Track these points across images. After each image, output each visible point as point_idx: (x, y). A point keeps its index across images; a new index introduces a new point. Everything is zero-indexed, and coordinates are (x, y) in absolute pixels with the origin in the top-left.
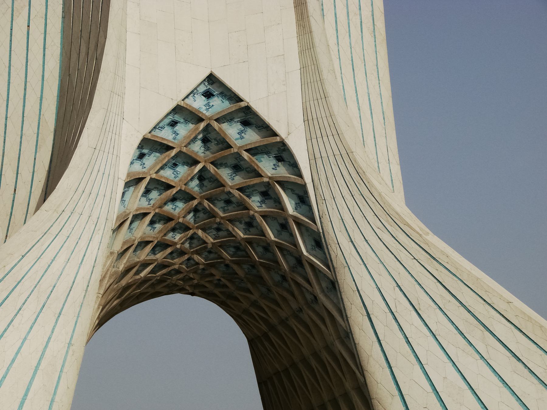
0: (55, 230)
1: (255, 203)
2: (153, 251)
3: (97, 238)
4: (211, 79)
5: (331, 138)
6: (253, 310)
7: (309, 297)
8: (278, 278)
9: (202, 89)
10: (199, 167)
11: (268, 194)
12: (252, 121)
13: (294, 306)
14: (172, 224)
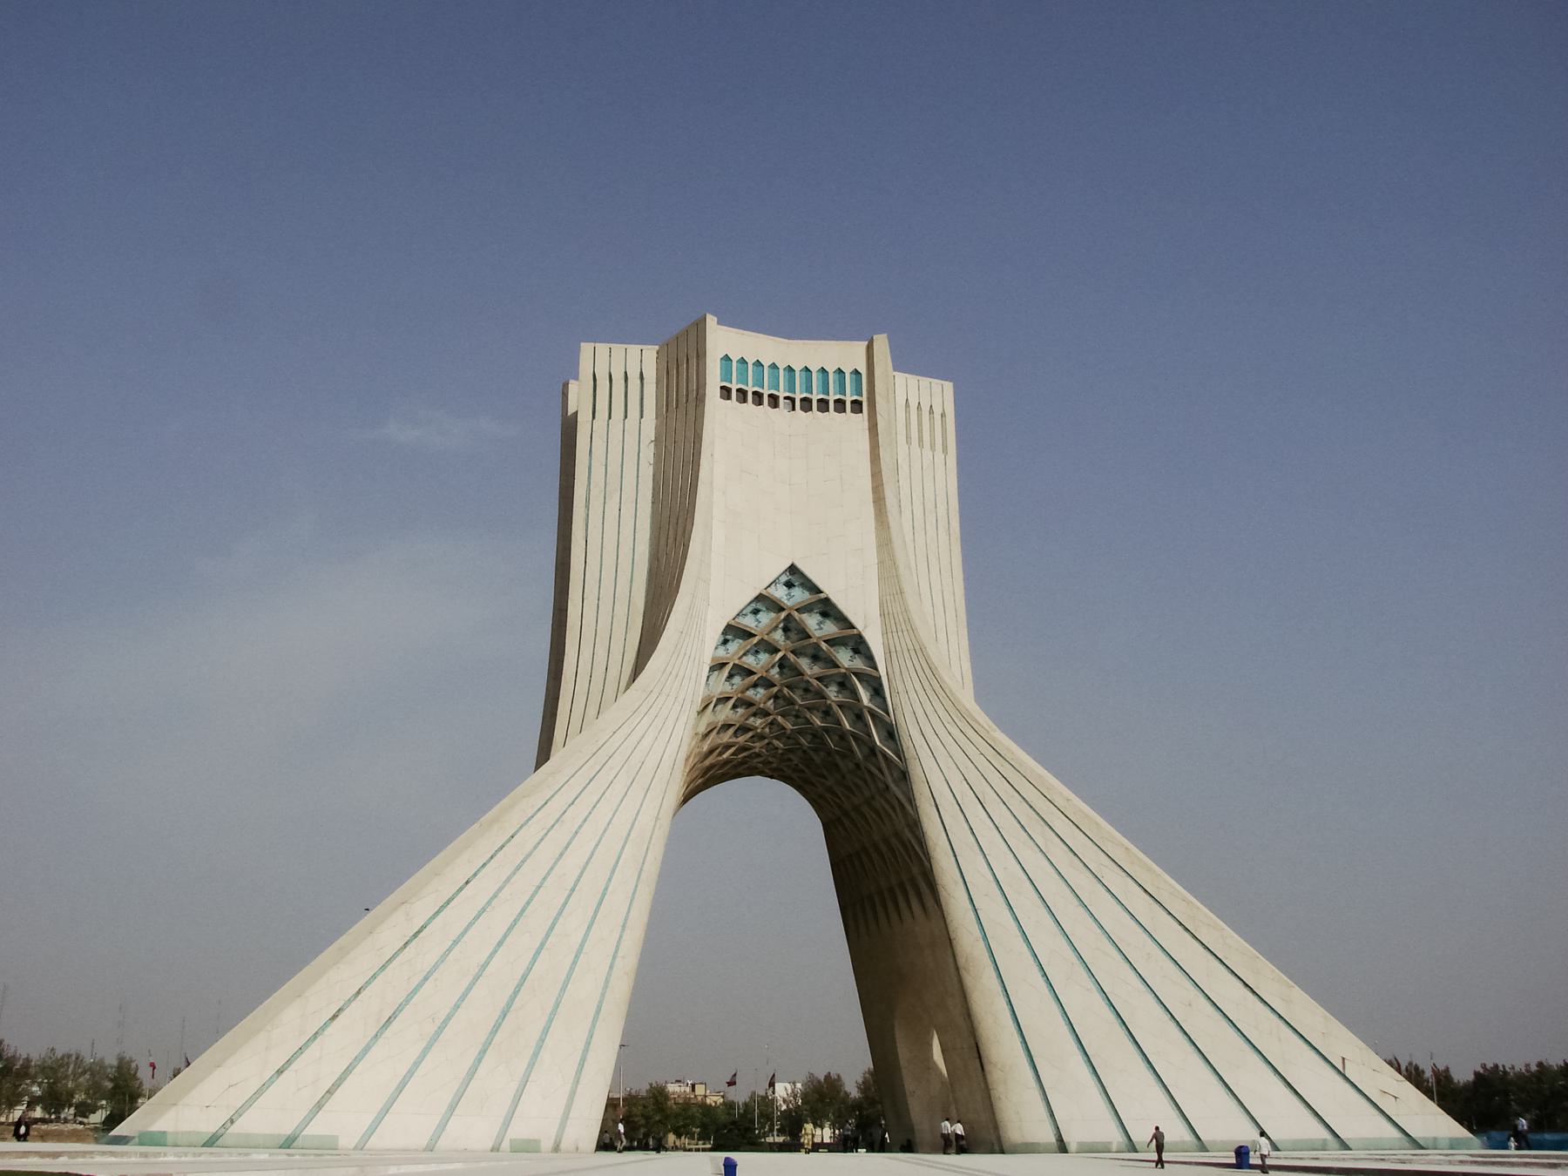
0: (644, 709)
1: (832, 692)
2: (735, 734)
3: (683, 719)
4: (793, 569)
6: (828, 795)
7: (881, 786)
8: (851, 766)
9: (784, 579)
10: (780, 655)
11: (844, 684)
13: (867, 794)
14: (753, 709)
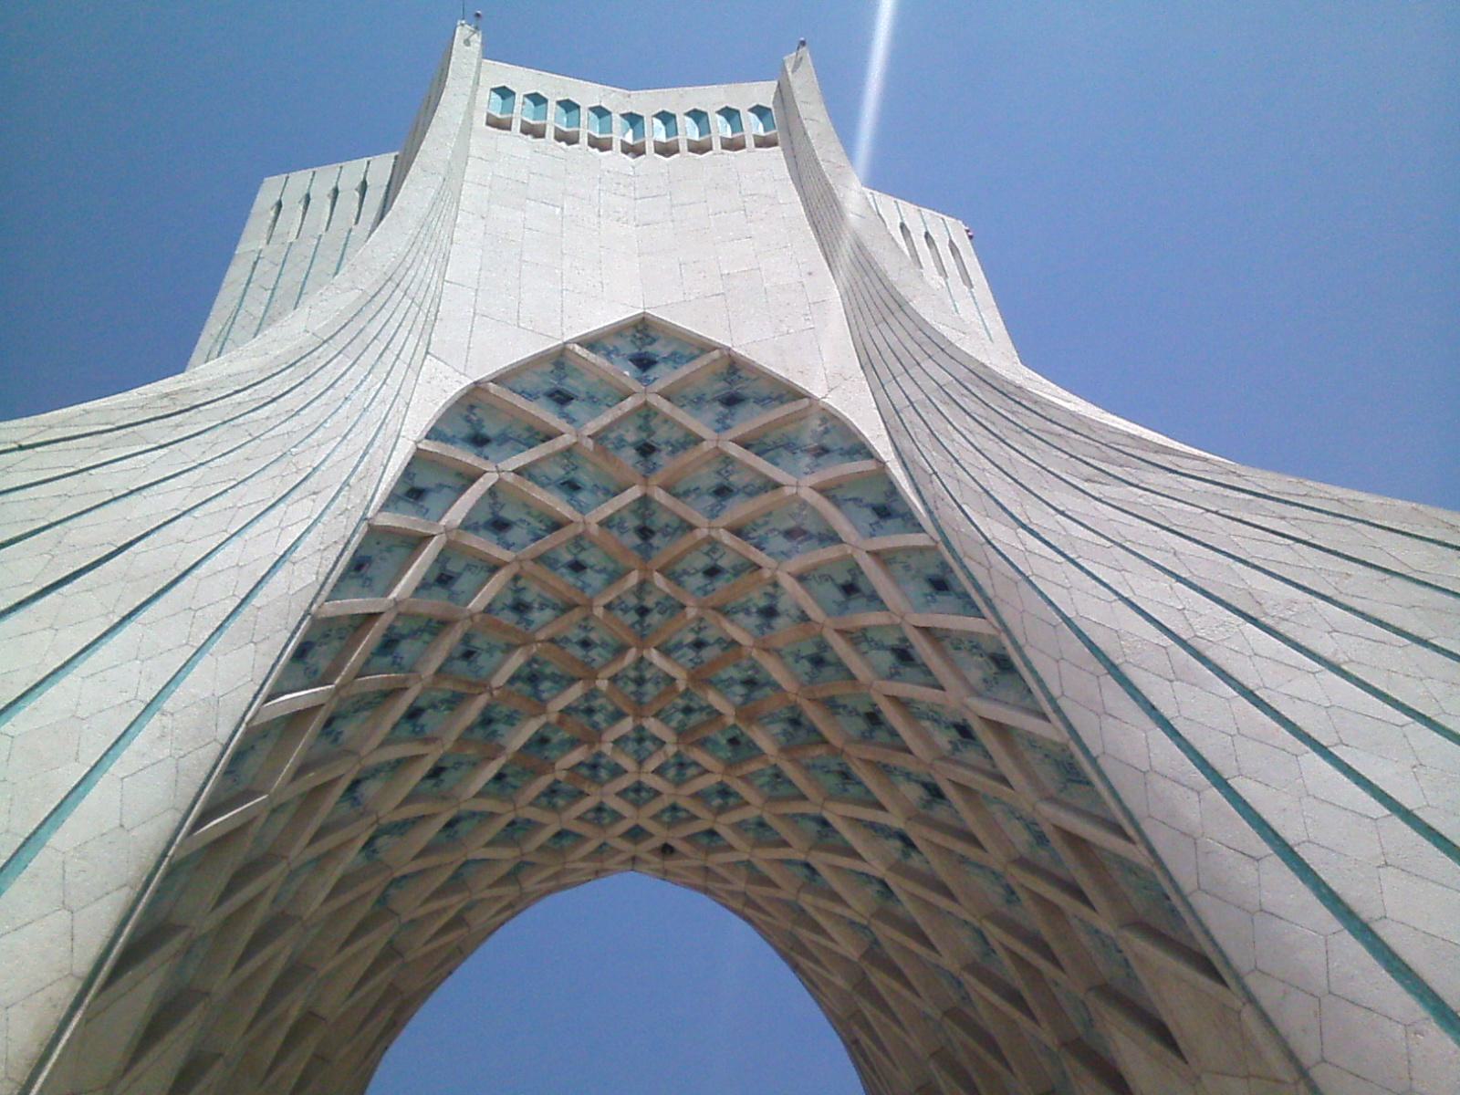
5: (927, 364)
12: (746, 392)
